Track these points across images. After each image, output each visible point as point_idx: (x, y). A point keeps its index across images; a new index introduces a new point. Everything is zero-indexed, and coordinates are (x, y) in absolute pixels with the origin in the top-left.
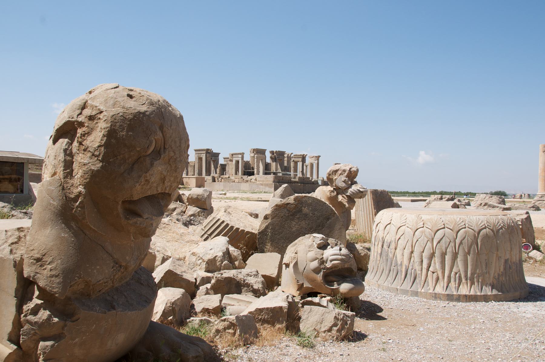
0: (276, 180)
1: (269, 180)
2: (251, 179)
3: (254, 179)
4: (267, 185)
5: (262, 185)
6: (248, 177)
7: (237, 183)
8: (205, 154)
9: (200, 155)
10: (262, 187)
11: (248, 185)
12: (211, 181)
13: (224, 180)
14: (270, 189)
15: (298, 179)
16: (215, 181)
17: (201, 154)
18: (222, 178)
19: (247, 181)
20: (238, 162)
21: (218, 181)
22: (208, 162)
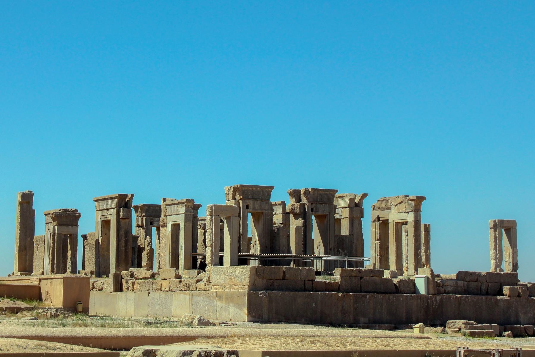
0: (260, 282)
1: (239, 281)
2: (198, 281)
3: (205, 279)
4: (230, 299)
5: (219, 297)
6: (199, 273)
7: (163, 294)
8: (115, 210)
9: (105, 212)
10: (218, 303)
11: (188, 297)
12: (112, 287)
13: (139, 284)
14: (237, 310)
15: (342, 276)
16: (121, 290)
17: (108, 209)
18: (137, 279)
19: (188, 287)
20: (176, 227)
21: (128, 289)
22: (122, 233)
